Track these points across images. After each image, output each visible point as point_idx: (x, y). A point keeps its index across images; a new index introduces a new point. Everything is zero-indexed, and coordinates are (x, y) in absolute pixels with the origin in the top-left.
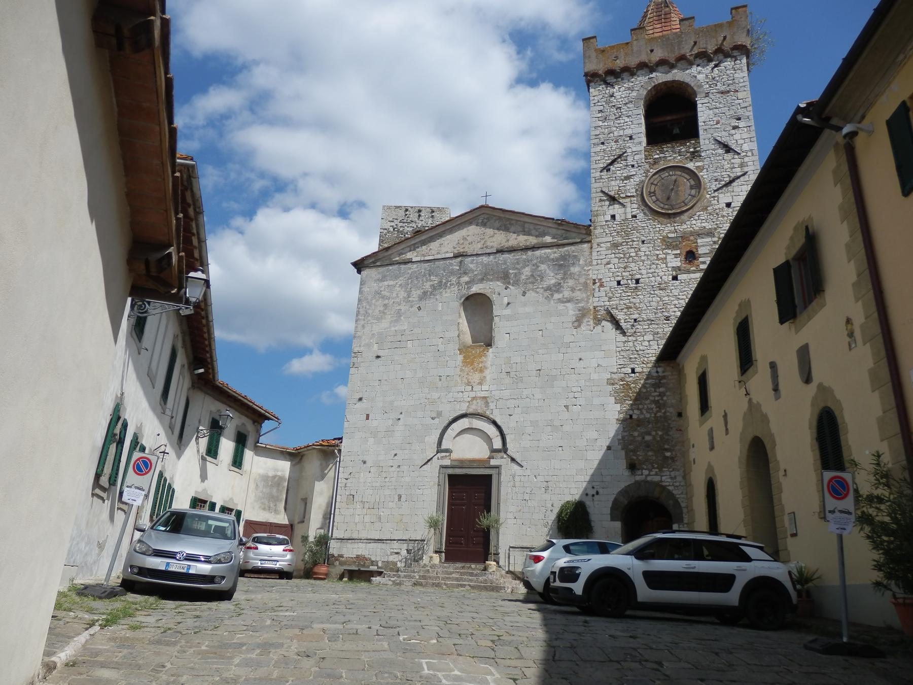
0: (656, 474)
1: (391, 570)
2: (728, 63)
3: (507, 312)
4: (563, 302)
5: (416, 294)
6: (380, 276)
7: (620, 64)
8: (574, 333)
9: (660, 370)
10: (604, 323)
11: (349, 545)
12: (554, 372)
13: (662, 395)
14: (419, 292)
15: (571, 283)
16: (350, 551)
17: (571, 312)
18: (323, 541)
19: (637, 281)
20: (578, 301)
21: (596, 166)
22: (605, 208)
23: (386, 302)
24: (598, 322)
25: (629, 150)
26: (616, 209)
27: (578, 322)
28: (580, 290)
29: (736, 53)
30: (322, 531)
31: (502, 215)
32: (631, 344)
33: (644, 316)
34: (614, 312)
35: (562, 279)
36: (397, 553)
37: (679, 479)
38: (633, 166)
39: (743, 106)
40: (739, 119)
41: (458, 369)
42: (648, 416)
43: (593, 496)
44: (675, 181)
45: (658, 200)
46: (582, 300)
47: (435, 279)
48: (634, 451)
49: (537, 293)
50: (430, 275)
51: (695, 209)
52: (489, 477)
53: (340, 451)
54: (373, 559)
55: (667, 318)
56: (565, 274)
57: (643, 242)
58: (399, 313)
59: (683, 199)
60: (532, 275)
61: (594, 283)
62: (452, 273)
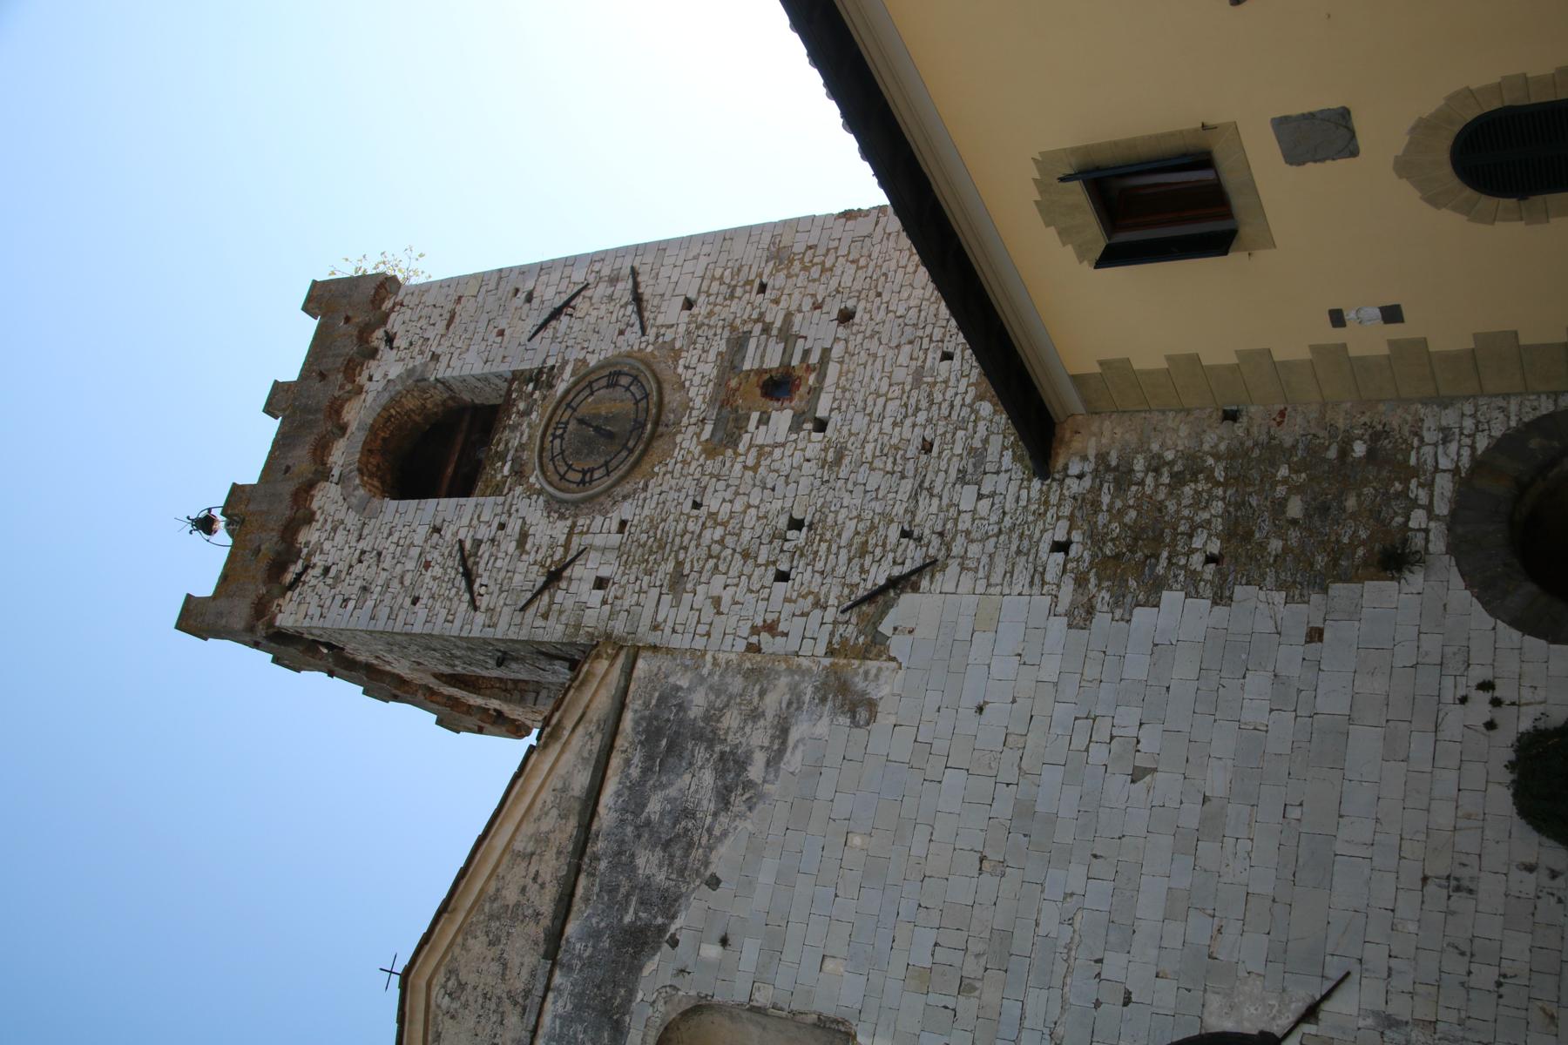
0: (1430, 485)
2: (395, 323)
3: (749, 952)
4: (781, 751)
8: (893, 720)
9: (1074, 469)
10: (885, 628)
12: (1003, 809)
15: (731, 720)
17: (822, 728)
19: (796, 524)
20: (795, 702)
21: (458, 623)
22: (569, 604)
24: (875, 646)
25: (461, 535)
26: (584, 573)
27: (858, 708)
28: (762, 694)
29: (387, 305)
31: (460, 918)
32: (974, 549)
33: (899, 509)
34: (861, 593)
35: (710, 747)
37: (1449, 418)
38: (502, 526)
40: (517, 290)
42: (1218, 507)
43: (1496, 702)
44: (581, 421)
45: (606, 464)
46: (793, 688)
49: (725, 834)
51: (666, 375)
55: (927, 447)
56: (699, 737)
57: (696, 505)
59: (630, 405)
60: (666, 846)
61: (754, 649)
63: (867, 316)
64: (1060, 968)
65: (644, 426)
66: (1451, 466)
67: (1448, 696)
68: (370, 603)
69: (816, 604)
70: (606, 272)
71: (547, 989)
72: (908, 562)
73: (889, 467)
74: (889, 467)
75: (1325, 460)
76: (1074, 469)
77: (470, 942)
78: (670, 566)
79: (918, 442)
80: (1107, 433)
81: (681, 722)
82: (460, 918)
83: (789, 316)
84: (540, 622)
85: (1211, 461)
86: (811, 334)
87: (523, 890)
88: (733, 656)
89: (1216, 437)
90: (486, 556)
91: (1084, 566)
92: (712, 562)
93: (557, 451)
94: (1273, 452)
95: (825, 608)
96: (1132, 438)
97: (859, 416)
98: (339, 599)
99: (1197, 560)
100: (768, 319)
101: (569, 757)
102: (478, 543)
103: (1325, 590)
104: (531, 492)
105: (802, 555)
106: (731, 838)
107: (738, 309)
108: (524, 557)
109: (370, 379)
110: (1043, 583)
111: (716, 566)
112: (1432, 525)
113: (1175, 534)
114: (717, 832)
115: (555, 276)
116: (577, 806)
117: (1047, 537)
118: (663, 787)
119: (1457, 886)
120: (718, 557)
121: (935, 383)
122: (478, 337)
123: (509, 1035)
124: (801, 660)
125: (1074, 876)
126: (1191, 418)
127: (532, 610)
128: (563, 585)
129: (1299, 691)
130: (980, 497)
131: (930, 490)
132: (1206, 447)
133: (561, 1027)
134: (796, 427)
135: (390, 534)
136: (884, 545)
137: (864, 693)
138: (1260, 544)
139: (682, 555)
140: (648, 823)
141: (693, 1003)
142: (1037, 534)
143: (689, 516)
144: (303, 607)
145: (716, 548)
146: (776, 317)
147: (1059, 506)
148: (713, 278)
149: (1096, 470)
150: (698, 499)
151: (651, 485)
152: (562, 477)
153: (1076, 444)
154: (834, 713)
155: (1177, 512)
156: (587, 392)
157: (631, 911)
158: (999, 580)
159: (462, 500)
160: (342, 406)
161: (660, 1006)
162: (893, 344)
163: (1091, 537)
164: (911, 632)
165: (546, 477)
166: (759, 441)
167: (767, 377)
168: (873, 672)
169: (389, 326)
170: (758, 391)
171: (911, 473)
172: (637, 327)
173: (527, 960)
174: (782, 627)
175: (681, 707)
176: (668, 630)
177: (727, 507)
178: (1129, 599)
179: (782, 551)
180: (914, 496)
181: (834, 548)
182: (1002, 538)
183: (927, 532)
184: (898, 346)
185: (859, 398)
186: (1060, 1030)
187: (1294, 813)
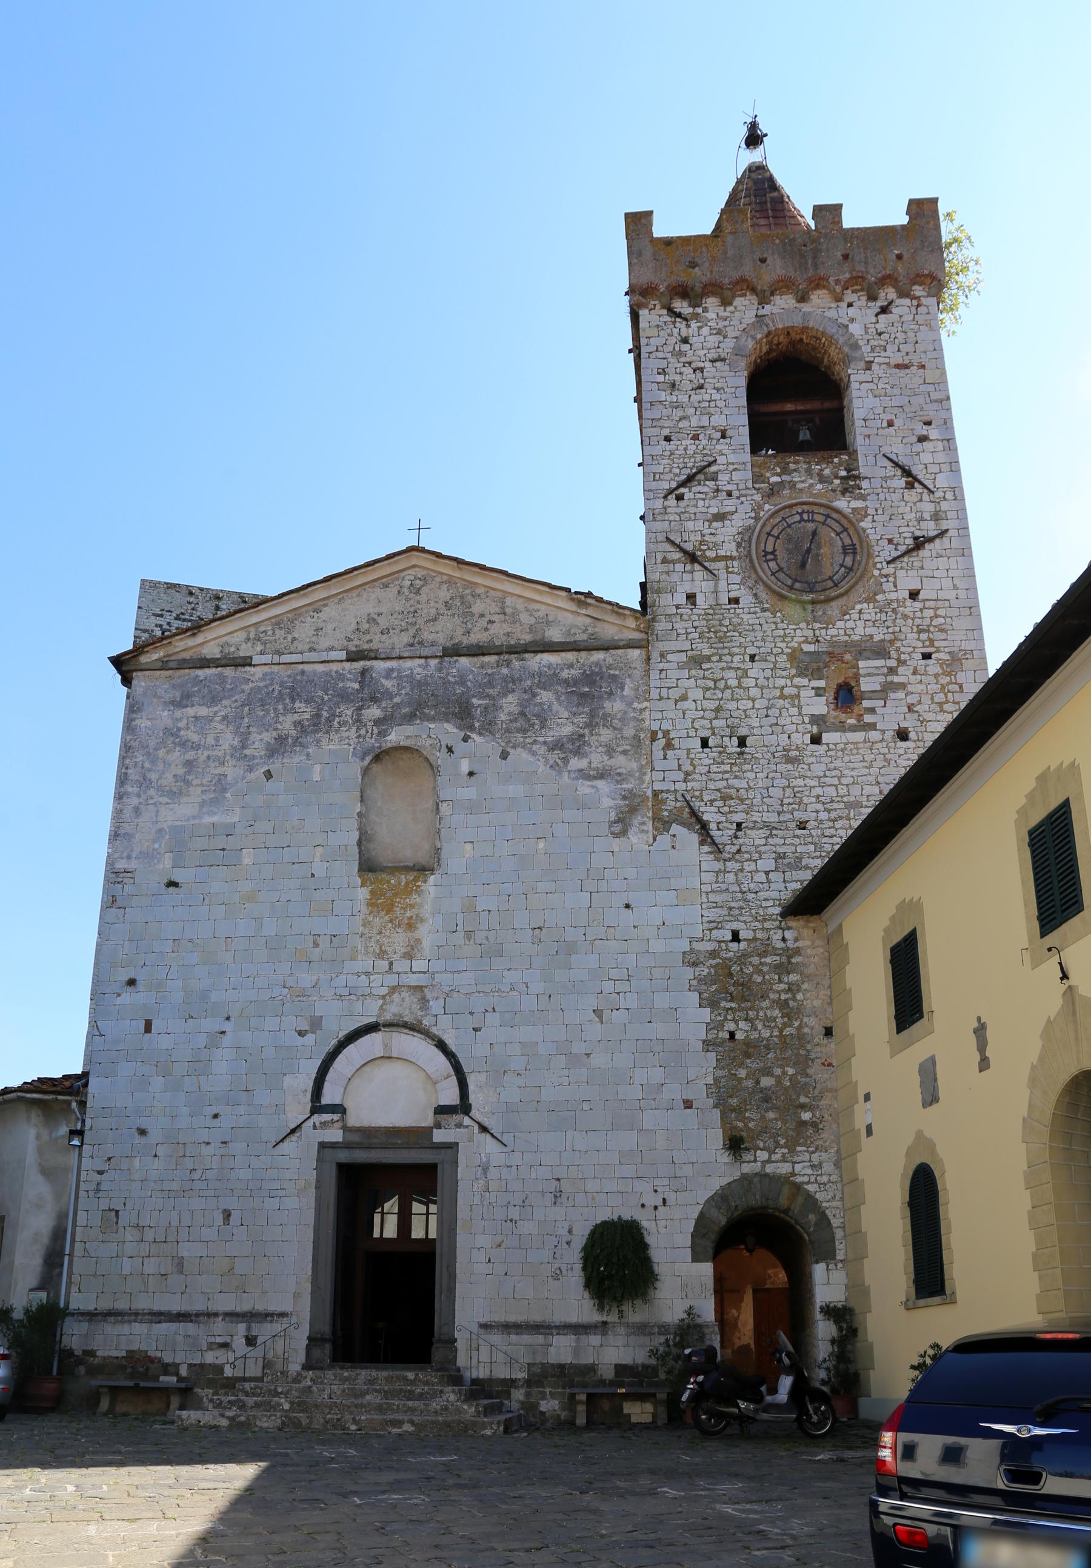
1: (211, 1383)
3: (468, 793)
4: (589, 778)
5: (260, 740)
6: (178, 695)
7: (699, 276)
8: (616, 850)
9: (788, 935)
10: (675, 828)
11: (110, 1329)
12: (571, 935)
13: (792, 989)
14: (268, 736)
15: (605, 735)
16: (113, 1342)
17: (607, 802)
18: (48, 1318)
19: (742, 742)
20: (621, 778)
22: (675, 577)
23: (191, 755)
24: (662, 824)
25: (721, 460)
26: (697, 581)
27: (621, 825)
28: (625, 752)
29: (918, 290)
30: (43, 1295)
31: (457, 574)
32: (731, 877)
33: (756, 817)
34: (696, 804)
35: (587, 725)
36: (225, 1346)
38: (729, 494)
39: (934, 396)
41: (359, 920)
42: (766, 1033)
44: (814, 533)
45: (781, 569)
46: (630, 774)
47: (304, 711)
48: (739, 1111)
49: (534, 754)
50: (293, 701)
51: (854, 596)
52: (432, 1168)
53: (82, 1104)
54: (168, 1358)
55: (802, 826)
56: (592, 715)
57: (752, 658)
58: (221, 785)
59: (828, 572)
60: (522, 714)
61: (654, 739)
62: (344, 696)
63: (902, 751)
64: (487, 988)
65: (812, 591)
66: (796, 1171)
67: (657, 1182)
68: (663, 396)
69: (687, 774)
70: (944, 506)
71: (426, 657)
72: (720, 833)
73: (786, 801)
74: (786, 801)
75: (799, 1095)
76: (788, 935)
77: (445, 586)
78: (706, 652)
79: (804, 817)
80: (814, 952)
81: (601, 698)
82: (457, 574)
83: (903, 686)
84: (659, 557)
85: (796, 1024)
86: (889, 709)
87: (482, 616)
88: (647, 723)
89: (813, 1025)
90: (706, 489)
91: (724, 955)
92: (711, 684)
93: (790, 521)
94: (803, 1063)
95: (685, 781)
96: (811, 970)
97: (823, 767)
98: (663, 364)
99: (731, 1026)
100: (901, 670)
101: (568, 619)
102: (715, 479)
103: (715, 1106)
104: (757, 509)
105: (720, 753)
106: (532, 759)
107: (911, 643)
108: (707, 524)
109: (850, 305)
110: (710, 930)
111: (708, 689)
112: (759, 1164)
113: (746, 1009)
114: (535, 747)
115: (941, 457)
116: (538, 637)
117: (741, 926)
118: (558, 699)
119: (557, 1197)
120: (715, 688)
121: (849, 819)
122: (887, 402)
123: (395, 639)
124: (649, 774)
125: (537, 987)
126: (826, 1006)
127: (668, 547)
128: (688, 567)
129: (654, 1100)
130: (767, 873)
131: (771, 835)
132: (806, 1020)
133: (406, 676)
134: (815, 719)
135: (718, 389)
136: (730, 812)
137: (631, 825)
138: (743, 1063)
139: (714, 659)
140: (534, 695)
141: (434, 764)
142: (742, 918)
143: (743, 655)
144: (654, 332)
145: (721, 685)
146: (904, 675)
147: (763, 929)
148: (936, 609)
149: (788, 949)
150: (757, 658)
151: (768, 614)
152: (769, 534)
153: (806, 932)
154: (617, 807)
155: (762, 1008)
156: (839, 529)
157: (480, 702)
158: (711, 899)
159: (748, 448)
160: (824, 287)
161: (429, 742)
162: (880, 779)
163: (743, 955)
164: (673, 847)
165: (768, 520)
166: (803, 693)
167: (853, 684)
168: (645, 828)
169: (899, 301)
170: (841, 680)
171: (782, 819)
172: (895, 554)
173: (441, 635)
174: (670, 753)
175: (611, 694)
176: (661, 666)
177: (752, 683)
178: (704, 987)
179: (722, 737)
180: (766, 825)
181: (727, 776)
182: (739, 895)
183: (741, 841)
184: (878, 783)
185: (838, 763)
186: (455, 995)
187: (586, 1106)
